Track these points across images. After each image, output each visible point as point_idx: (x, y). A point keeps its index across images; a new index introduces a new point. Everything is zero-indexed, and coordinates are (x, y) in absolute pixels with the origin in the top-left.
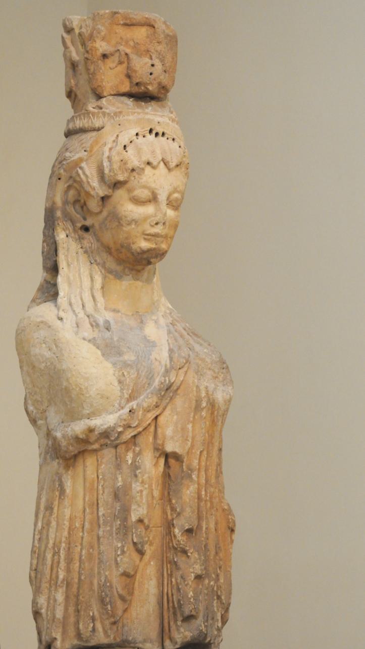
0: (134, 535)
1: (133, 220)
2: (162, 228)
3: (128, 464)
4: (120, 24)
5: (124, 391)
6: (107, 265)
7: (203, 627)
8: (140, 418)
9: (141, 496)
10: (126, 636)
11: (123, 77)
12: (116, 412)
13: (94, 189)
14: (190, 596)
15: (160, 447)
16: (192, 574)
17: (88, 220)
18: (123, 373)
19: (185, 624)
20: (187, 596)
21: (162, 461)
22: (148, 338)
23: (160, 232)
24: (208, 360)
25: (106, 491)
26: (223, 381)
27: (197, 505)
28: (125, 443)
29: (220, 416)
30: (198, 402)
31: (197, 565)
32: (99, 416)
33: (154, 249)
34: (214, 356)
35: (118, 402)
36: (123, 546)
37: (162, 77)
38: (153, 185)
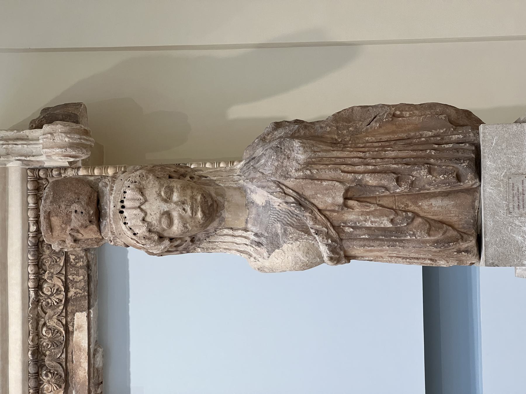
4: (52, 234)
6: (216, 226)
9: (375, 222)
11: (87, 230)
13: (166, 247)
19: (462, 178)
21: (351, 203)
24: (276, 164)
25: (372, 244)
26: (290, 150)
28: (339, 235)
30: (306, 178)
36: (411, 235)
38: (158, 215)
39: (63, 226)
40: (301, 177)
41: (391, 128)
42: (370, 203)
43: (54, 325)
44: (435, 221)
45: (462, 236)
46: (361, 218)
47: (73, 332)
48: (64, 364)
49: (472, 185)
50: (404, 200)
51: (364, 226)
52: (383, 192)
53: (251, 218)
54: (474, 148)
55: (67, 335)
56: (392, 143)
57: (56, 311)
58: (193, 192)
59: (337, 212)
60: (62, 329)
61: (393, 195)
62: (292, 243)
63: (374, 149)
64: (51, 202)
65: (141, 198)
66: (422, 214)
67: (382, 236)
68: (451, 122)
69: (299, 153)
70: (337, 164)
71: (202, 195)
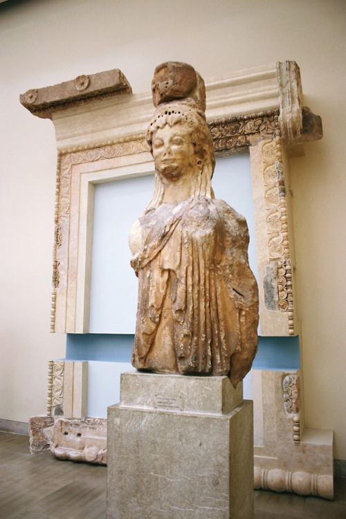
21: (166, 275)
24: (195, 217)
33: (168, 167)
38: (161, 137)
41: (230, 307)
44: (154, 339)
45: (144, 359)
54: (207, 371)
64: (174, 66)
66: (159, 329)
70: (194, 263)
71: (178, 167)
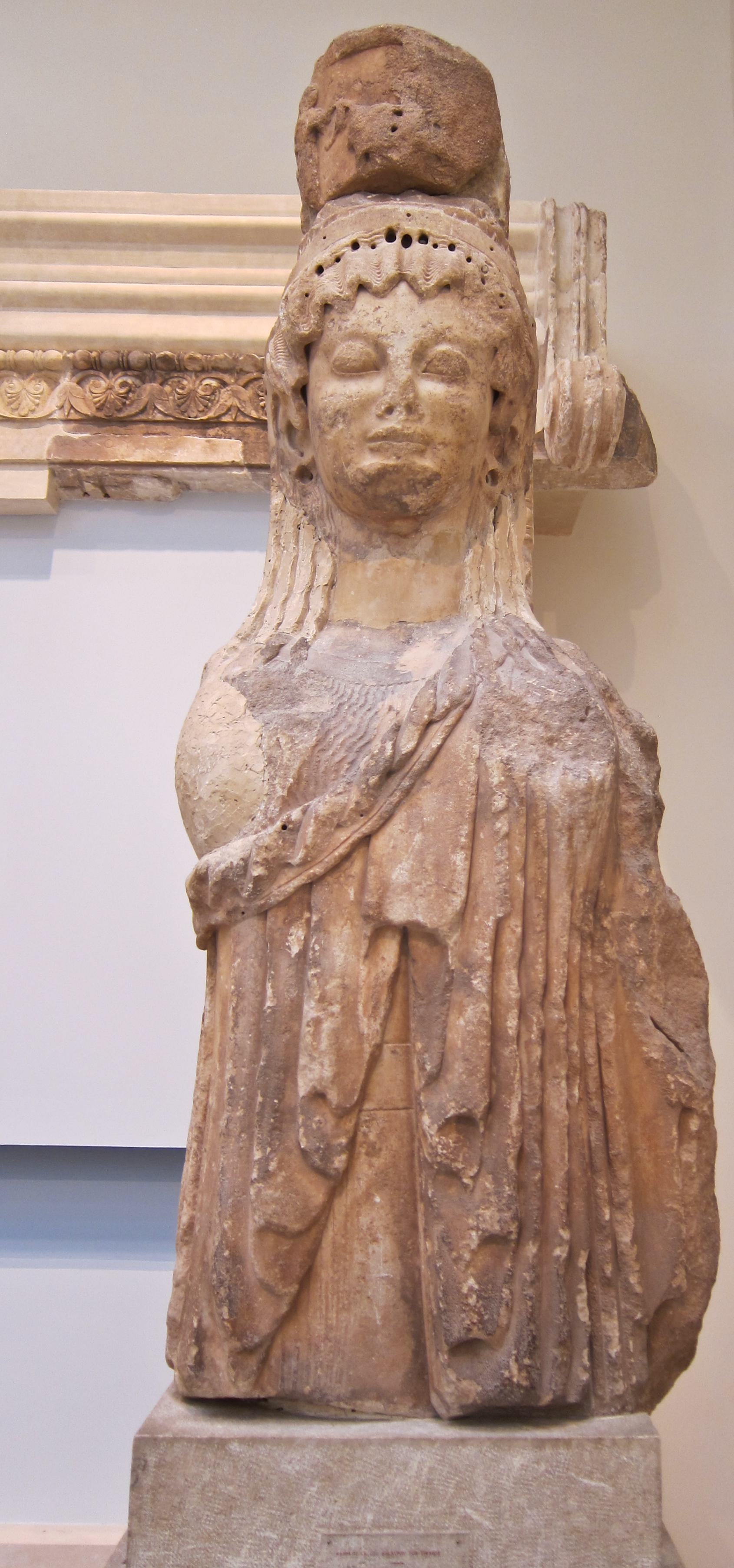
0: (302, 1130)
1: (338, 412)
2: (402, 417)
3: (290, 954)
5: (276, 782)
7: (515, 1371)
8: (309, 841)
9: (316, 1035)
10: (294, 1383)
11: (344, 154)
12: (256, 833)
13: (279, 377)
14: (465, 1290)
15: (371, 913)
16: (474, 1234)
17: (305, 454)
18: (278, 740)
20: (459, 1290)
21: (390, 950)
22: (398, 668)
23: (399, 427)
24: (531, 701)
25: (244, 1021)
27: (485, 1053)
28: (280, 904)
29: (560, 830)
31: (487, 1208)
32: (225, 844)
33: (396, 469)
34: (553, 691)
35: (263, 807)
37: (424, 133)
38: (374, 330)
39: (358, 87)
40: (483, 779)
42: (386, 1018)
43: (222, 401)
44: (313, 1253)
46: (333, 985)
47: (204, 436)
48: (143, 417)
49: (440, 1395)
50: (393, 1142)
51: (306, 995)
52: (422, 1068)
53: (360, 635)
54: (573, 1398)
55: (199, 426)
56: (596, 1103)
57: (249, 404)
58: (444, 444)
59: (359, 902)
60: (211, 414)
61: (412, 1104)
62: (260, 746)
63: (574, 1037)
64: (429, 52)
65: (432, 283)
67: (268, 1059)
68: (663, 1307)
69: (566, 776)
70: (529, 905)
71: (437, 476)
